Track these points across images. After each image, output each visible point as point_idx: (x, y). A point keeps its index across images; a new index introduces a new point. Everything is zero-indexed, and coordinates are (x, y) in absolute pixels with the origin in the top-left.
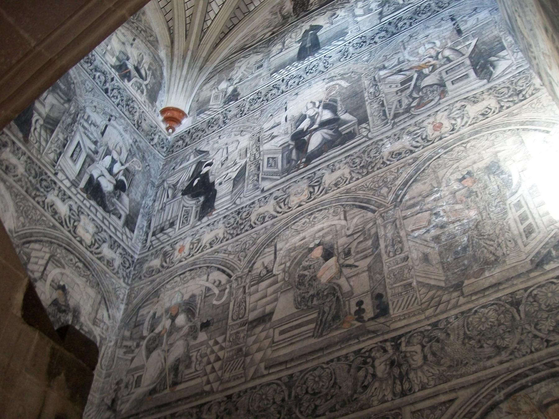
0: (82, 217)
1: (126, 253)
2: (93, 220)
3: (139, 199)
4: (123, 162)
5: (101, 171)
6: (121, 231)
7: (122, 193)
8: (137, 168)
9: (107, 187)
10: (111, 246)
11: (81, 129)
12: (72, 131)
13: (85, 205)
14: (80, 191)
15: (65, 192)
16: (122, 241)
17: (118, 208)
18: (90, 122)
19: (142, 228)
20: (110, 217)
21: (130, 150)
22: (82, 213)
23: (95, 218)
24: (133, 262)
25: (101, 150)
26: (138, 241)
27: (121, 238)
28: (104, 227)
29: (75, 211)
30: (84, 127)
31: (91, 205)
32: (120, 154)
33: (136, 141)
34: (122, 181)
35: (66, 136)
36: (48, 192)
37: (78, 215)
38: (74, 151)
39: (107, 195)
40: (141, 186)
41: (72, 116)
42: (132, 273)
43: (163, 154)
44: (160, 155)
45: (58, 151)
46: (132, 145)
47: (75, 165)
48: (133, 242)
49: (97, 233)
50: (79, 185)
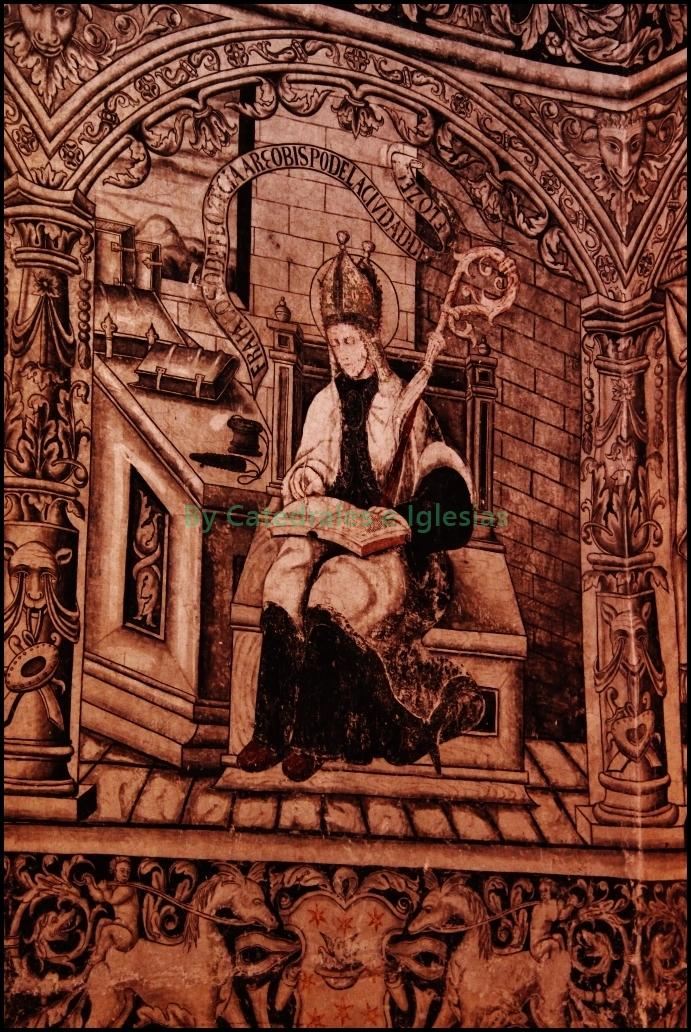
0: (301, 920)
1: (581, 893)
2: (363, 872)
3: (556, 493)
4: (405, 349)
5: (312, 536)
6: (519, 793)
7: (456, 555)
8: (490, 307)
9: (372, 601)
10: (495, 925)
11: (115, 376)
12: (73, 440)
13: (298, 833)
14: (239, 777)
15: (165, 863)
16: (543, 844)
17: (466, 667)
18: (146, 279)
19: (620, 659)
20: (438, 765)
21: (423, 229)
22: (297, 892)
23: (369, 856)
24: (628, 913)
25: (265, 407)
26: (619, 761)
27: (531, 835)
28: (427, 860)
29: (256, 927)
30: (130, 349)
31: (327, 798)
32: (368, 320)
33: (440, 120)
34: (442, 474)
35: (53, 518)
36: (82, 964)
37: (283, 932)
38: (131, 559)
39: (380, 648)
40: (545, 411)
41: (36, 353)
42: (644, 994)
43: (620, 51)
44: (599, 81)
45: (48, 653)
46: (420, 180)
47: (165, 644)
48: (597, 791)
49: (401, 937)
50: (223, 746)
